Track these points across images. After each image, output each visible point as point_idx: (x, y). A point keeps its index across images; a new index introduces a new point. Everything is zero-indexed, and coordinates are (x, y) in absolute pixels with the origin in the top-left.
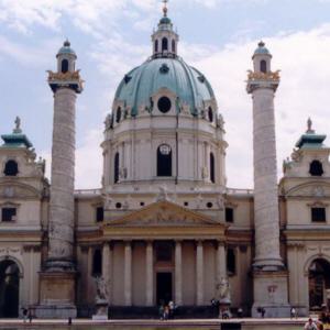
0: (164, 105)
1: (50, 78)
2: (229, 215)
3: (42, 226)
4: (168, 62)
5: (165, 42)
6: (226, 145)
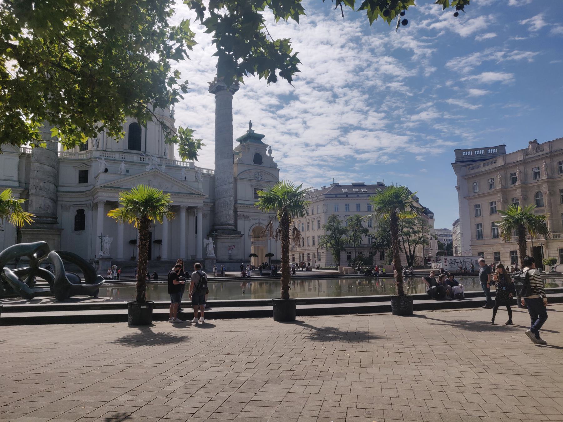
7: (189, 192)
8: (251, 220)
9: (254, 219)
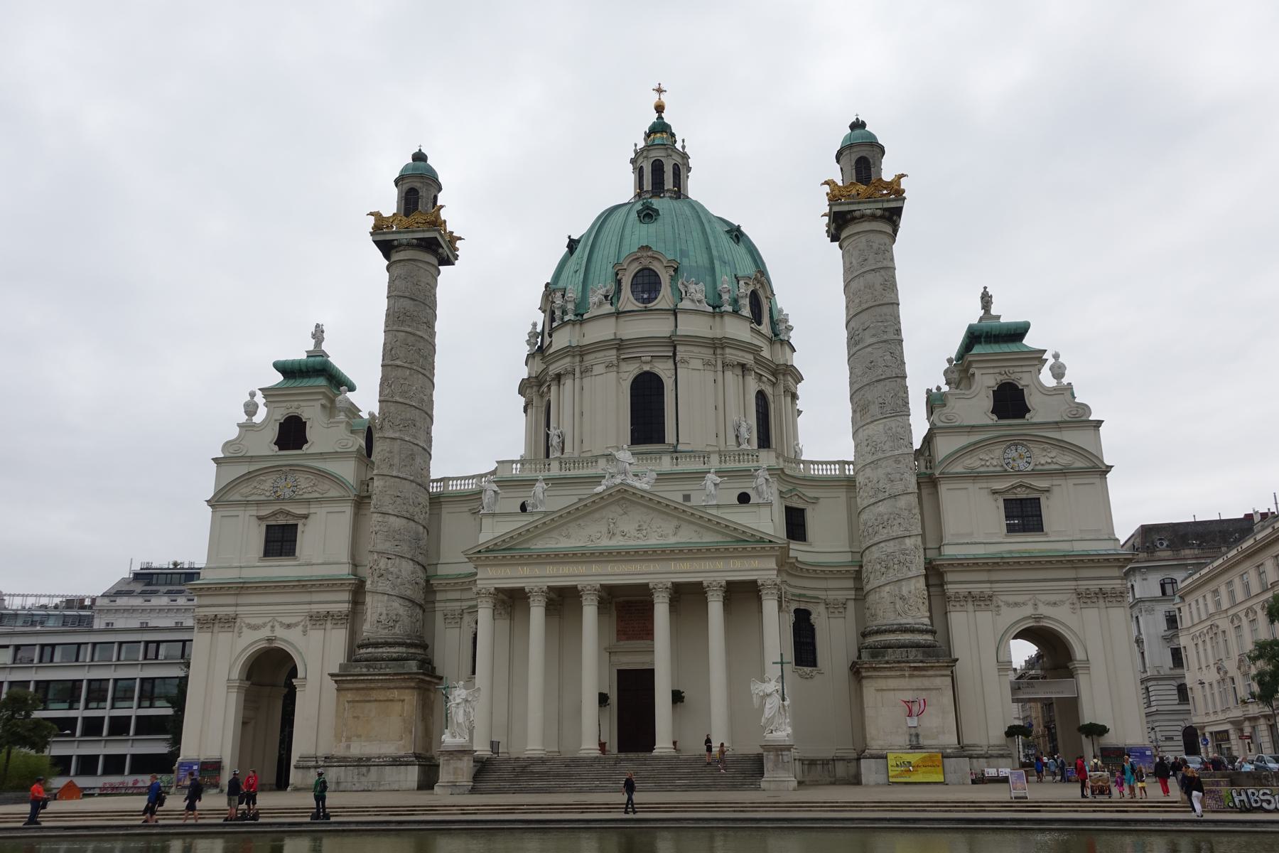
0: (647, 283)
1: (377, 230)
2: (796, 524)
3: (355, 565)
4: (656, 203)
5: (658, 168)
6: (798, 378)
7: (729, 539)
8: (1004, 609)
9: (1016, 604)
